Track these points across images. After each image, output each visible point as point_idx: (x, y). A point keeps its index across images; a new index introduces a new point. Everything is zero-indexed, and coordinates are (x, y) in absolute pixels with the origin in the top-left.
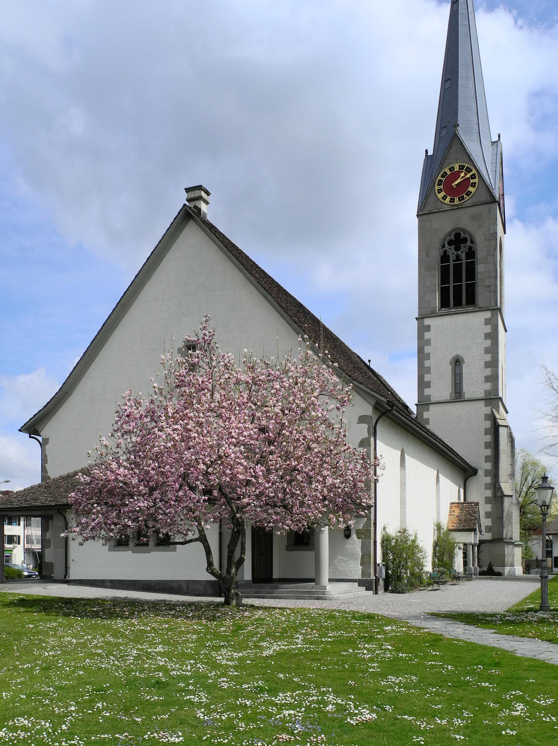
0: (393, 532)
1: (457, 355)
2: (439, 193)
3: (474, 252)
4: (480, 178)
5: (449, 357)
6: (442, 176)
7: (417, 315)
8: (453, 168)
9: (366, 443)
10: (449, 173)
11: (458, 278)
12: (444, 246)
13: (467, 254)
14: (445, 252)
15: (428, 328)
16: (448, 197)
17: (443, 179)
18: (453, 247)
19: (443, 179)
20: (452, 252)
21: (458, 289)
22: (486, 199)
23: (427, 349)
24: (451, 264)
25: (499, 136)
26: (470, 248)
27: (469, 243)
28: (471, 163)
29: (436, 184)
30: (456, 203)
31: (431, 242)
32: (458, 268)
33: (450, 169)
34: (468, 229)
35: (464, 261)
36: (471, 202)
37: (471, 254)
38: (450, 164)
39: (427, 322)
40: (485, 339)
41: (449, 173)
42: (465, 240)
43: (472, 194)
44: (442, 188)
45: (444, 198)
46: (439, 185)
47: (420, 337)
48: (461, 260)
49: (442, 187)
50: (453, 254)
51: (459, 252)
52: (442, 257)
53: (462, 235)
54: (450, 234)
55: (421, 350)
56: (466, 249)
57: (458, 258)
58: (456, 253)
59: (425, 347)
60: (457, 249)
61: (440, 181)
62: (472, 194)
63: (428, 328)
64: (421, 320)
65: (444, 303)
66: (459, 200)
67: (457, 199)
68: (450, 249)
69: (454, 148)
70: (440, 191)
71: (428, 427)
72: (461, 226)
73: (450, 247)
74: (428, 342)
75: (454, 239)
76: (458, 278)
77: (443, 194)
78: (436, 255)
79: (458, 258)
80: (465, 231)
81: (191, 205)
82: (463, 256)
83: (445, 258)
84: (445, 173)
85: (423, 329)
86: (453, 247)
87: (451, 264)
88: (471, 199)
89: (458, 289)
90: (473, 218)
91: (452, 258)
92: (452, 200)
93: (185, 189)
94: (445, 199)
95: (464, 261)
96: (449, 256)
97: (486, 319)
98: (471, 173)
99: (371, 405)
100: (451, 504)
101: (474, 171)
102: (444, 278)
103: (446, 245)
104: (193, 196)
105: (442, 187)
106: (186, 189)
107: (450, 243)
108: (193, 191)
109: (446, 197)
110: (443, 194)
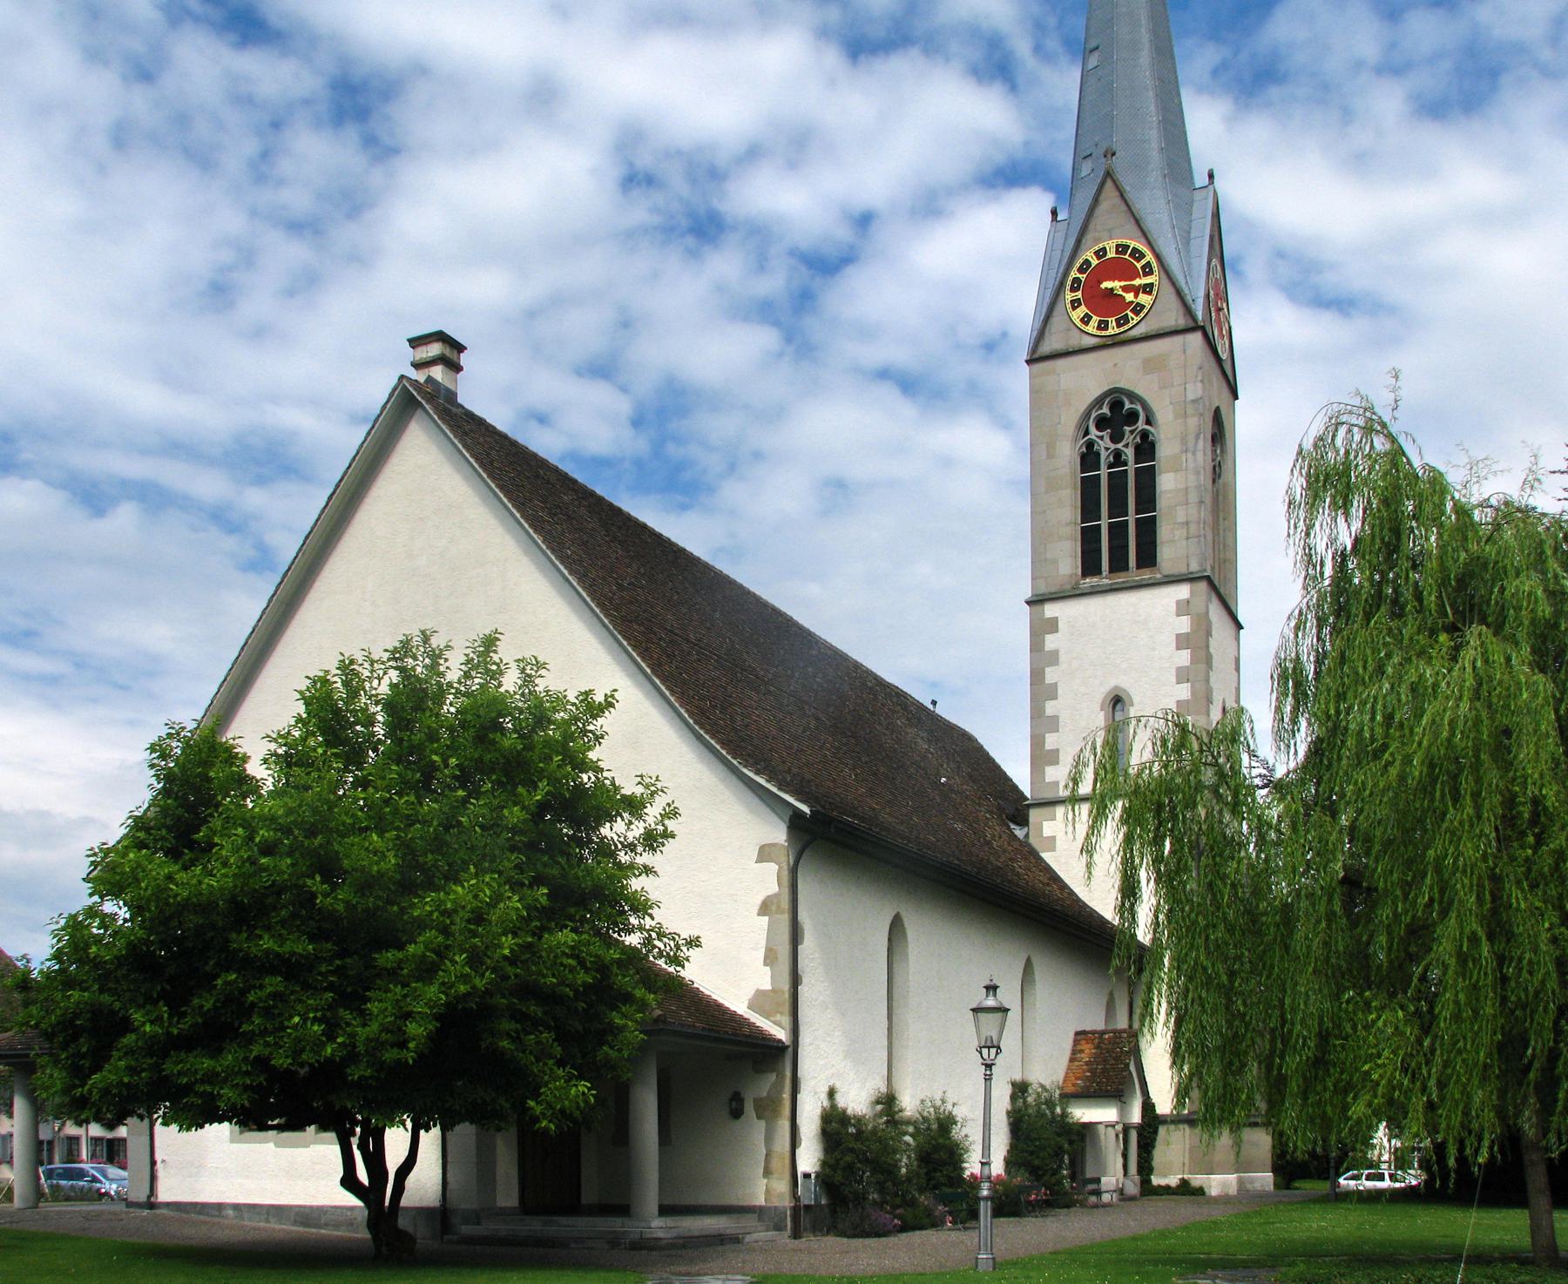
0: (857, 1100)
1: (1116, 688)
2: (1074, 308)
3: (1152, 446)
5: (1101, 692)
6: (1081, 270)
7: (1028, 594)
8: (1104, 250)
9: (774, 908)
10: (1095, 262)
11: (1118, 506)
12: (1087, 433)
13: (1138, 448)
14: (1090, 444)
15: (1053, 625)
16: (1095, 318)
17: (1083, 277)
18: (1106, 434)
19: (1083, 277)
20: (1104, 445)
21: (1118, 531)
22: (1176, 320)
23: (1051, 675)
24: (1104, 472)
25: (1211, 176)
26: (1145, 435)
27: (1141, 425)
28: (1143, 240)
29: (1068, 287)
30: (1110, 332)
31: (1059, 423)
32: (1118, 482)
33: (1096, 253)
34: (1139, 391)
35: (1131, 467)
37: (1146, 448)
38: (1097, 241)
39: (1050, 610)
40: (1178, 648)
41: (1095, 262)
42: (1132, 417)
43: (1145, 311)
44: (1080, 296)
45: (1086, 320)
46: (1073, 290)
47: (1036, 645)
49: (1079, 294)
50: (1107, 449)
51: (1120, 446)
52: (1083, 457)
53: (1127, 405)
54: (1098, 402)
55: (1037, 676)
56: (1135, 438)
57: (1118, 458)
58: (1113, 447)
59: (1048, 670)
61: (1076, 280)
62: (1145, 311)
63: (1053, 625)
64: (1037, 608)
65: (1090, 565)
66: (1119, 325)
67: (1112, 321)
68: (1101, 438)
69: (1104, 206)
70: (1075, 304)
71: (1046, 856)
72: (1121, 385)
73: (1101, 434)
74: (1054, 658)
76: (1118, 506)
77: (1082, 310)
78: (1067, 454)
79: (1118, 458)
80: (1133, 397)
81: (420, 376)
82: (1129, 453)
83: (1089, 458)
84: (1087, 262)
85: (1041, 629)
86: (1106, 434)
87: (1104, 472)
88: (1143, 323)
89: (1118, 531)
90: (1149, 365)
92: (1103, 326)
93: (408, 340)
94: (1087, 323)
95: (1131, 467)
96: (1098, 455)
97: (1178, 603)
98: (1143, 262)
99: (784, 821)
100: (1077, 1034)
101: (1149, 257)
102: (1089, 508)
103: (1094, 433)
104: (424, 356)
105: (1079, 294)
107: (1101, 423)
108: (426, 344)
110: (1082, 310)
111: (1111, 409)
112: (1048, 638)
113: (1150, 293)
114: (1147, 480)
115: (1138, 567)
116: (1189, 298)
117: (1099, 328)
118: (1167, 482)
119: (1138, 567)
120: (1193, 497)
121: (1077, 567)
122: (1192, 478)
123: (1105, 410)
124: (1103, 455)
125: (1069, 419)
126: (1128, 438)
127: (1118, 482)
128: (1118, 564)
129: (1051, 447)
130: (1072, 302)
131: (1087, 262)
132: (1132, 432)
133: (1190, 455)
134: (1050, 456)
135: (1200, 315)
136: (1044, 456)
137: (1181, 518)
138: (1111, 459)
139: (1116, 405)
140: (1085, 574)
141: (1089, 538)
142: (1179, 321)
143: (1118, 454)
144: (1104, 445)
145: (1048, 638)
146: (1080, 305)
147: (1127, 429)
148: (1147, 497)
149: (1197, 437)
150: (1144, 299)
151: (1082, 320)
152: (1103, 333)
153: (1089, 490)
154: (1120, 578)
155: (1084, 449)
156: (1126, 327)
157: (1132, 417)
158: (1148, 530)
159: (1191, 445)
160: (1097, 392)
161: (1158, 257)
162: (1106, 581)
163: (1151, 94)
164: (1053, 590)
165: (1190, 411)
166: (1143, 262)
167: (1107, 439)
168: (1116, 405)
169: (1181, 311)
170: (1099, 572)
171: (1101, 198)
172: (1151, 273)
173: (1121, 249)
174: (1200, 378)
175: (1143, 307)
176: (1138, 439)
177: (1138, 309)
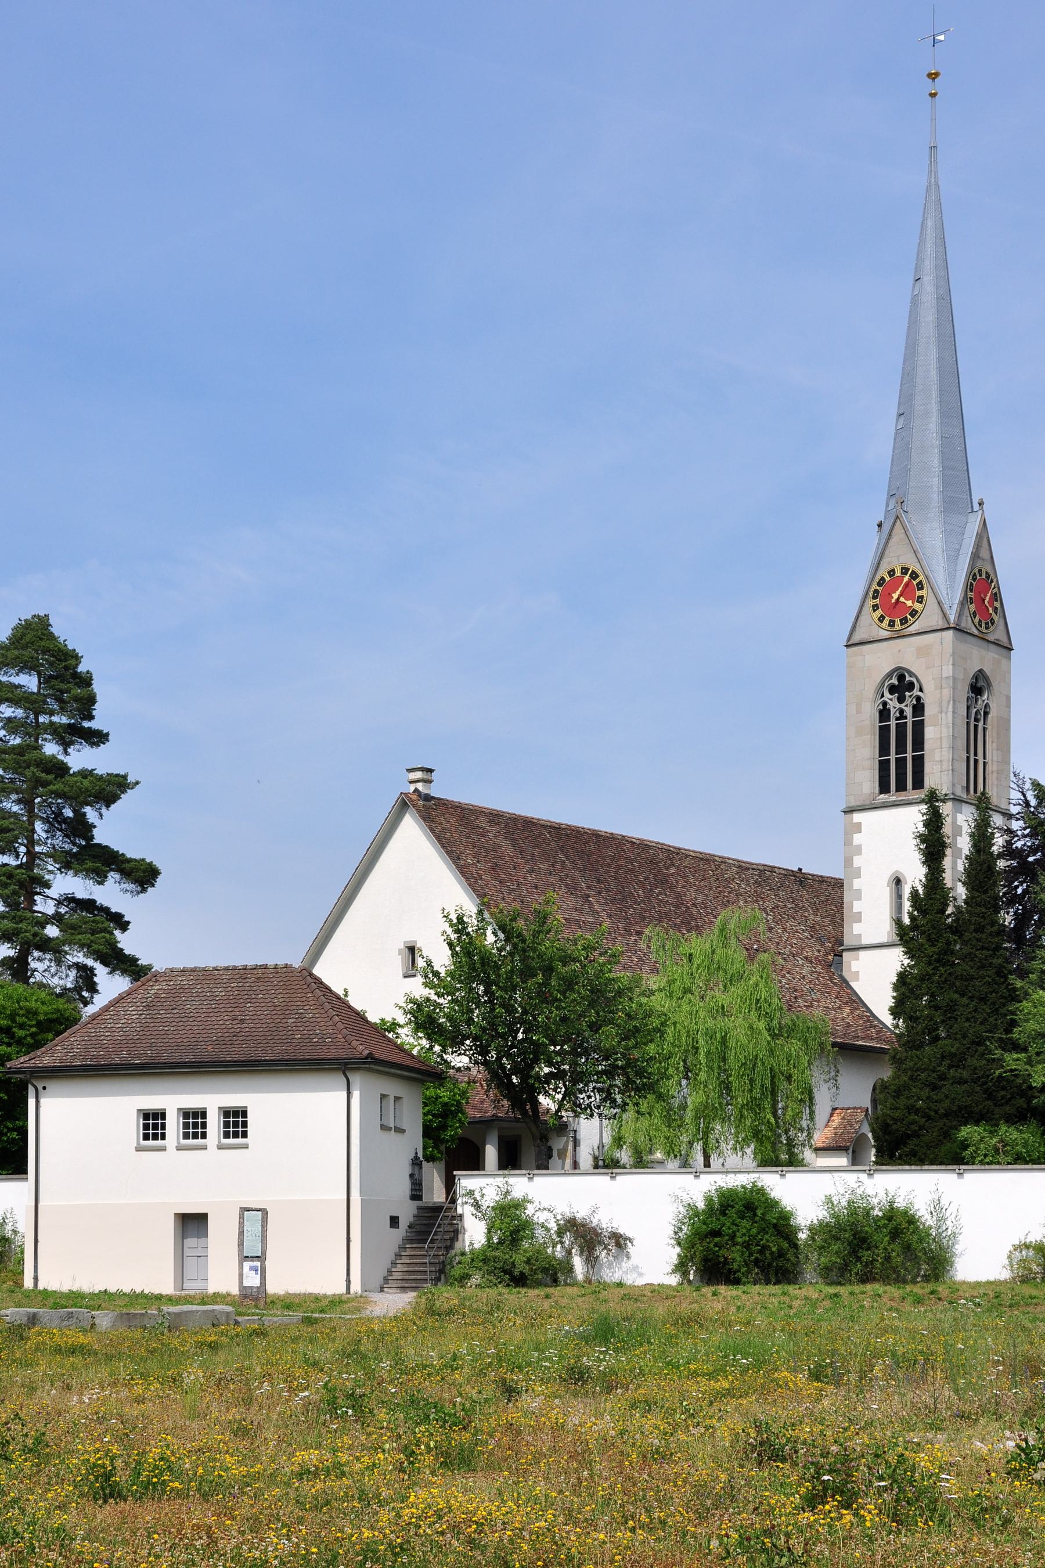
1: (897, 871)
2: (874, 611)
3: (923, 705)
4: (929, 589)
6: (879, 584)
7: (843, 807)
11: (901, 747)
12: (883, 696)
13: (914, 707)
14: (885, 704)
20: (893, 704)
21: (901, 763)
24: (893, 723)
26: (918, 698)
27: (916, 692)
32: (901, 729)
35: (909, 721)
36: (917, 628)
37: (919, 708)
39: (857, 817)
41: (888, 579)
42: (911, 686)
45: (881, 619)
46: (874, 598)
48: (906, 718)
51: (902, 706)
52: (881, 712)
53: (908, 678)
54: (889, 675)
58: (898, 706)
60: (901, 700)
62: (918, 614)
63: (858, 828)
64: (848, 816)
65: (884, 788)
67: (898, 622)
68: (891, 700)
70: (875, 608)
74: (858, 850)
75: (897, 683)
76: (901, 747)
77: (879, 612)
78: (870, 713)
80: (911, 674)
82: (908, 711)
83: (884, 713)
84: (883, 579)
87: (893, 723)
90: (921, 652)
91: (894, 714)
92: (892, 624)
95: (909, 721)
96: (889, 710)
98: (918, 580)
102: (884, 749)
103: (887, 695)
105: (877, 601)
106: (165, 1150)
107: (892, 689)
109: (884, 618)
110: (879, 612)
111: (899, 680)
112: (856, 836)
113: (921, 602)
114: (919, 728)
115: (913, 789)
116: (946, 607)
117: (889, 625)
118: (929, 733)
119: (913, 789)
120: (946, 744)
121: (874, 788)
122: (944, 730)
123: (894, 681)
124: (893, 711)
125: (870, 688)
126: (908, 700)
127: (901, 729)
128: (901, 787)
129: (859, 706)
130: (874, 606)
131: (883, 579)
132: (910, 696)
133: (943, 714)
134: (858, 712)
135: (952, 618)
136: (854, 712)
137: (938, 758)
138: (898, 715)
139: (901, 678)
140: (881, 792)
141: (884, 766)
142: (941, 624)
143: (902, 711)
144: (893, 704)
145: (856, 836)
146: (878, 608)
147: (907, 694)
148: (919, 743)
149: (949, 702)
150: (918, 606)
151: (879, 619)
152: (892, 629)
153: (884, 732)
154: (902, 796)
155: (881, 707)
156: (906, 625)
157: (911, 686)
158: (919, 763)
159: (944, 709)
160: (887, 670)
161: (927, 577)
162: (894, 798)
163: (936, 451)
164: (858, 803)
165: (944, 685)
166: (918, 580)
167: (895, 700)
168: (901, 678)
169: (941, 615)
170: (889, 792)
171: (893, 535)
172: (922, 588)
173: (905, 570)
174: (951, 662)
175: (917, 612)
176: (914, 702)
177: (914, 613)
